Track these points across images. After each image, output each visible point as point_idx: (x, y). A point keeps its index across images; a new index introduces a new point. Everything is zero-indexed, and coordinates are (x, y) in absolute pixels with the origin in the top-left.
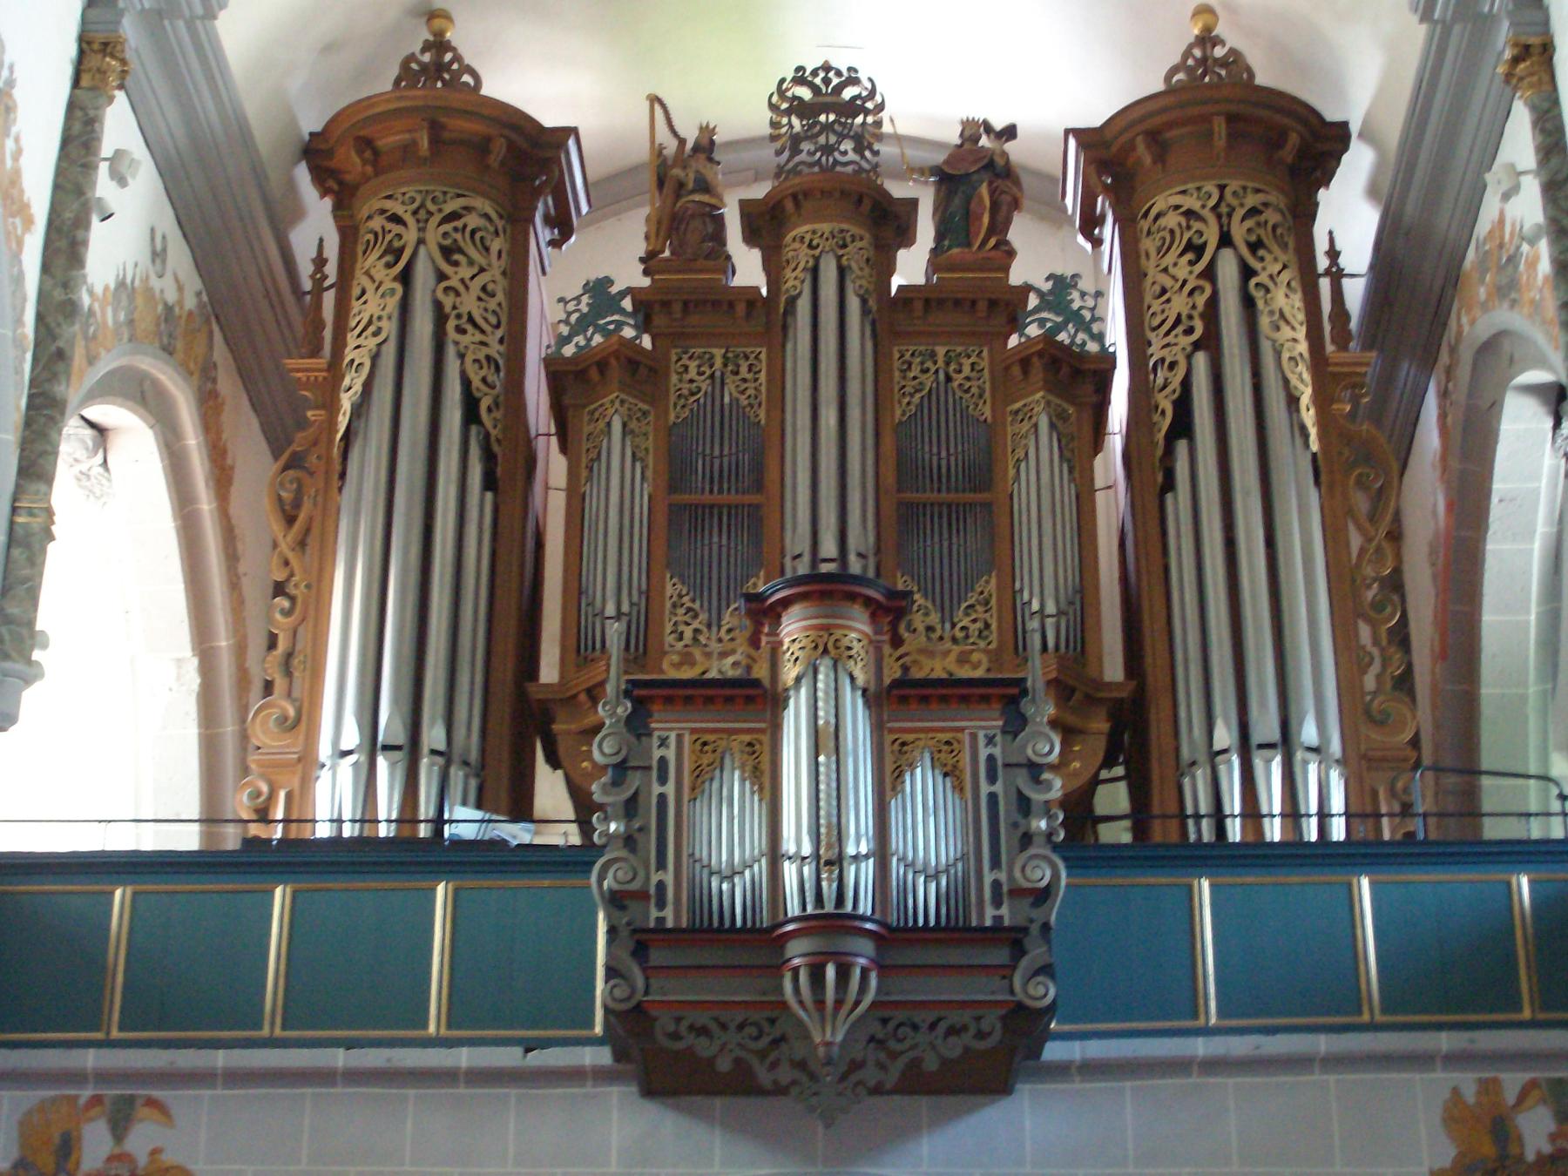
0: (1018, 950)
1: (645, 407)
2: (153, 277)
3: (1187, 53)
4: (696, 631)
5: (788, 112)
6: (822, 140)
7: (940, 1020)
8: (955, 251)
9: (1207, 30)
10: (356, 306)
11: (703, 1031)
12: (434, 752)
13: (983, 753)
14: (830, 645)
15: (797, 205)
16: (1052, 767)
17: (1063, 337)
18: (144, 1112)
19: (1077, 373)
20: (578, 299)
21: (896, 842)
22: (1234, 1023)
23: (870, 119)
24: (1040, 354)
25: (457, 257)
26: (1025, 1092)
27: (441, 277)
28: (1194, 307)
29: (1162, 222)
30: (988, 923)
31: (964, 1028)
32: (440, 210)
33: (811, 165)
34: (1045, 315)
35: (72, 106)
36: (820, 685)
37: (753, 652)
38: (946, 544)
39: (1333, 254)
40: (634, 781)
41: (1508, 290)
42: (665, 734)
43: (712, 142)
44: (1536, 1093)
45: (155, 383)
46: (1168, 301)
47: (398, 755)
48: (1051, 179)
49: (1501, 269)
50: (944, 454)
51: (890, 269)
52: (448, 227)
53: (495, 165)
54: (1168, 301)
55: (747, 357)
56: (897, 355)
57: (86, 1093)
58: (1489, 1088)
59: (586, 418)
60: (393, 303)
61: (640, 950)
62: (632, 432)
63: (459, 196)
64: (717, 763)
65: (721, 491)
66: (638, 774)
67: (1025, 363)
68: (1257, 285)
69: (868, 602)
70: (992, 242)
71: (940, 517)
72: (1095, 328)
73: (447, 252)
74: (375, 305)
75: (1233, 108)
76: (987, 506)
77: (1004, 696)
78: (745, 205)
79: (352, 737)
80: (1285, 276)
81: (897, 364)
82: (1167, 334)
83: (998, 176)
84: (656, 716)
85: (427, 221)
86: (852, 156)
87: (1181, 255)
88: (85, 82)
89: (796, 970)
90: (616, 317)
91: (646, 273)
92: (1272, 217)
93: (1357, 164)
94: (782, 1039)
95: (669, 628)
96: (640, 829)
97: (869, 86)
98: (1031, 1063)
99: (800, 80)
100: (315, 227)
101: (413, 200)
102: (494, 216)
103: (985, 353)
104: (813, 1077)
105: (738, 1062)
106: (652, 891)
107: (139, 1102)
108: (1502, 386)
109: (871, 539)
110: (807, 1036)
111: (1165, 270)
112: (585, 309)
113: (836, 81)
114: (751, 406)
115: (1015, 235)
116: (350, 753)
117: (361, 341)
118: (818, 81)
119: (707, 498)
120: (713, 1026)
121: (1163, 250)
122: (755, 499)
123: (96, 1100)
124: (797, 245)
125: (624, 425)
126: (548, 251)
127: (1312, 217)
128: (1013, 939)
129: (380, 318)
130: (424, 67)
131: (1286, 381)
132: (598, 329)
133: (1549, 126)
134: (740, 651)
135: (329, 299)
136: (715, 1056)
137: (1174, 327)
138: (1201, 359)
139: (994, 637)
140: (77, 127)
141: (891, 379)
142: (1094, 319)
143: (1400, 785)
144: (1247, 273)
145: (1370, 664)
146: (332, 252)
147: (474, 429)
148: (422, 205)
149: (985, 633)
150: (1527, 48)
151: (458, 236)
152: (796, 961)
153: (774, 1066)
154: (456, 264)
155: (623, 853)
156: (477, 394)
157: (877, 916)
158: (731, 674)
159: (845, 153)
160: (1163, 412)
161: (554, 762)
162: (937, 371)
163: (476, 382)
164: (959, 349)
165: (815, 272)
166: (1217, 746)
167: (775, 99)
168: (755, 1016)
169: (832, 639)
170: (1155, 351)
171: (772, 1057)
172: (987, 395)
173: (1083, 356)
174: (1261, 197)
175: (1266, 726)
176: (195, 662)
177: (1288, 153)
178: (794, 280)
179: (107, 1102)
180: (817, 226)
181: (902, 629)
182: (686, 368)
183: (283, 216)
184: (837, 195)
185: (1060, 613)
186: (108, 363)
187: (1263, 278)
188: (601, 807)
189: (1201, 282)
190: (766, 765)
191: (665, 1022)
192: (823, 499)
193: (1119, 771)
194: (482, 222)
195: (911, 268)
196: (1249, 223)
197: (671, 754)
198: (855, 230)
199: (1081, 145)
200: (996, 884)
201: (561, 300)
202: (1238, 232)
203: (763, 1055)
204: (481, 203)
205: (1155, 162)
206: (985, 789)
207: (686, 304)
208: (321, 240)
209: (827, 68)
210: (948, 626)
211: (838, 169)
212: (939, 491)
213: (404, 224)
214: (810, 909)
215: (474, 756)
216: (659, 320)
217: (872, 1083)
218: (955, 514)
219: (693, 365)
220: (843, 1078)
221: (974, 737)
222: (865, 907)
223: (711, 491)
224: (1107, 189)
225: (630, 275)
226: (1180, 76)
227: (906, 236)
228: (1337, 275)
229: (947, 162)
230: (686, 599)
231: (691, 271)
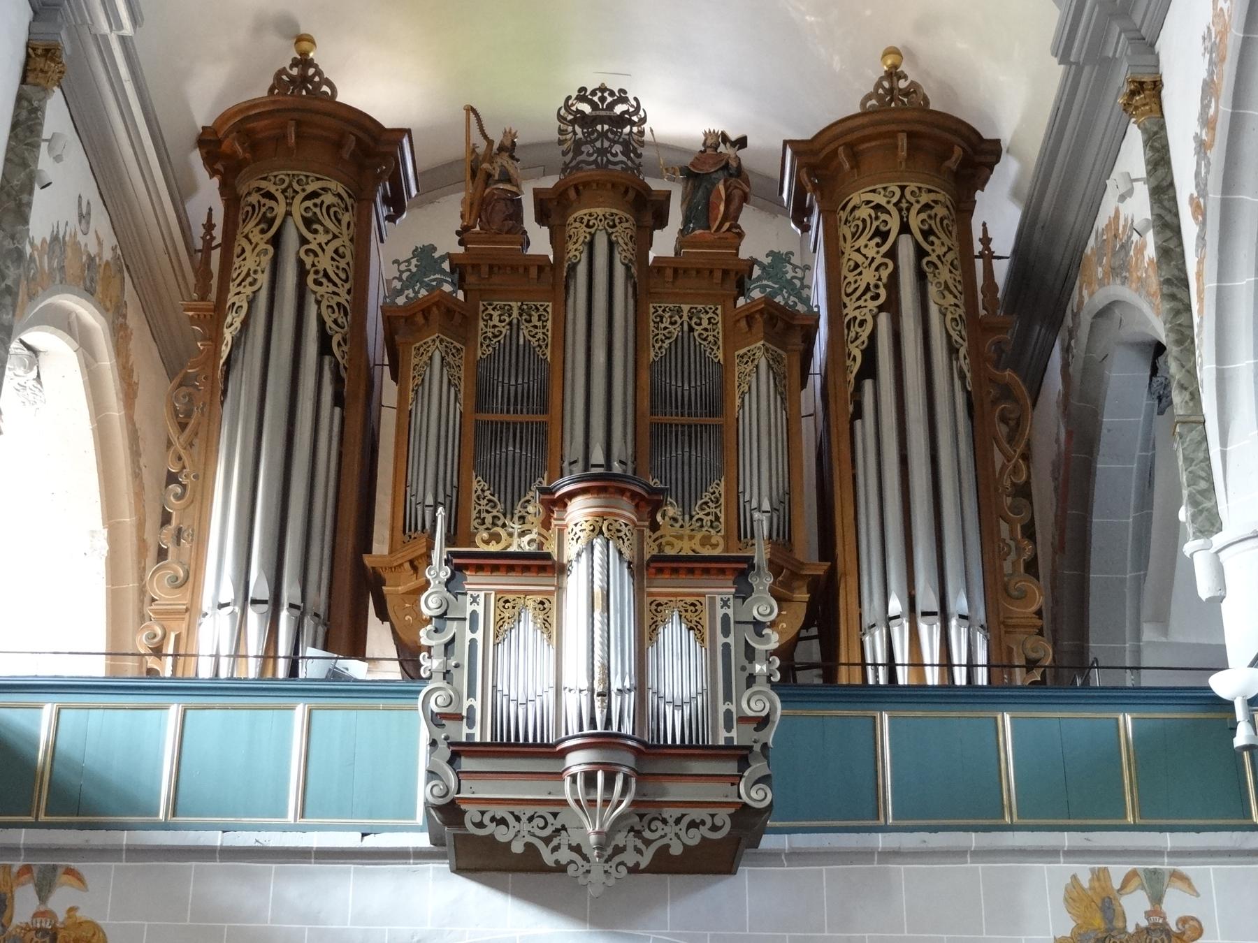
0: (744, 762)
1: (459, 346)
2: (80, 234)
3: (879, 85)
4: (494, 517)
5: (572, 123)
6: (598, 144)
7: (683, 815)
8: (698, 232)
9: (895, 67)
10: (237, 262)
11: (502, 822)
12: (292, 606)
13: (720, 612)
14: (604, 529)
15: (577, 192)
16: (773, 625)
17: (779, 299)
18: (65, 878)
19: (789, 327)
20: (408, 261)
21: (651, 681)
22: (905, 823)
23: (635, 129)
24: (761, 312)
25: (316, 226)
26: (744, 871)
27: (304, 241)
28: (880, 279)
29: (857, 213)
30: (722, 742)
31: (703, 823)
32: (304, 190)
34: (765, 282)
35: (20, 98)
36: (595, 558)
37: (544, 532)
38: (687, 455)
39: (986, 240)
40: (452, 628)
41: (1120, 270)
42: (475, 593)
43: (513, 144)
44: (1135, 882)
46: (860, 273)
47: (265, 607)
48: (769, 179)
49: (1115, 253)
50: (686, 387)
52: (309, 203)
53: (346, 156)
54: (860, 273)
55: (537, 309)
56: (653, 310)
57: (17, 864)
58: (1100, 876)
59: (414, 353)
60: (266, 261)
61: (453, 760)
62: (449, 364)
63: (318, 179)
64: (516, 617)
65: (515, 411)
66: (455, 623)
67: (750, 319)
68: (928, 263)
69: (634, 495)
70: (727, 225)
71: (683, 435)
72: (805, 292)
73: (308, 222)
76: (719, 428)
77: (735, 569)
78: (537, 193)
79: (227, 594)
80: (950, 256)
81: (652, 317)
82: (859, 299)
83: (731, 175)
84: (470, 579)
85: (293, 198)
86: (621, 157)
87: (870, 239)
88: (29, 80)
89: (574, 777)
90: (437, 276)
92: (940, 211)
93: (1007, 173)
94: (564, 828)
95: (474, 514)
96: (457, 666)
97: (634, 103)
98: (753, 850)
99: (582, 98)
101: (283, 181)
102: (345, 196)
103: (719, 312)
105: (529, 846)
106: (464, 714)
107: (60, 871)
109: (630, 451)
111: (858, 250)
112: (414, 270)
113: (609, 99)
114: (540, 346)
115: (741, 222)
116: (227, 605)
117: (240, 289)
118: (596, 99)
119: (505, 417)
120: (510, 819)
121: (856, 236)
122: (541, 418)
123: (27, 869)
124: (577, 224)
125: (443, 359)
126: (385, 225)
127: (971, 212)
128: (742, 756)
129: (255, 272)
130: (293, 80)
131: (949, 336)
132: (424, 285)
133: (1157, 145)
134: (535, 530)
135: (216, 255)
136: (510, 842)
137: (864, 294)
138: (884, 318)
139: (722, 526)
140: (24, 114)
141: (648, 326)
142: (803, 287)
143: (1028, 646)
144: (920, 253)
145: (1009, 554)
146: (218, 219)
147: (327, 359)
148: (290, 186)
149: (716, 524)
150: (1142, 83)
151: (317, 210)
152: (573, 770)
153: (556, 849)
154: (315, 232)
155: (443, 684)
156: (330, 332)
157: (636, 736)
158: (527, 549)
159: (615, 155)
160: (854, 359)
161: (383, 615)
162: (682, 324)
163: (329, 323)
164: (700, 307)
165: (591, 245)
166: (892, 613)
167: (563, 112)
168: (542, 810)
169: (606, 523)
170: (850, 312)
171: (555, 842)
172: (720, 343)
173: (794, 314)
174: (933, 196)
175: (927, 599)
176: (105, 532)
177: (952, 163)
178: (575, 250)
179: (35, 871)
180: (593, 210)
181: (659, 518)
182: (491, 316)
183: (181, 192)
184: (609, 186)
185: (774, 509)
188: (429, 649)
189: (886, 260)
190: (554, 621)
194: (336, 200)
195: (664, 244)
196: (923, 216)
197: (480, 610)
198: (621, 214)
199: (795, 153)
200: (728, 713)
201: (394, 262)
202: (915, 222)
203: (547, 841)
204: (334, 185)
205: (852, 168)
206: (721, 640)
207: (491, 267)
208: (210, 209)
209: (603, 89)
210: (687, 517)
211: (610, 167)
212: (682, 415)
213: (276, 200)
214: (586, 731)
215: (322, 610)
216: (471, 279)
217: (630, 864)
218: (694, 434)
219: (495, 314)
221: (712, 600)
222: (627, 729)
223: (508, 411)
224: (816, 188)
225: (449, 245)
226: (874, 102)
227: (661, 221)
228: (988, 256)
229: (692, 164)
230: (487, 493)
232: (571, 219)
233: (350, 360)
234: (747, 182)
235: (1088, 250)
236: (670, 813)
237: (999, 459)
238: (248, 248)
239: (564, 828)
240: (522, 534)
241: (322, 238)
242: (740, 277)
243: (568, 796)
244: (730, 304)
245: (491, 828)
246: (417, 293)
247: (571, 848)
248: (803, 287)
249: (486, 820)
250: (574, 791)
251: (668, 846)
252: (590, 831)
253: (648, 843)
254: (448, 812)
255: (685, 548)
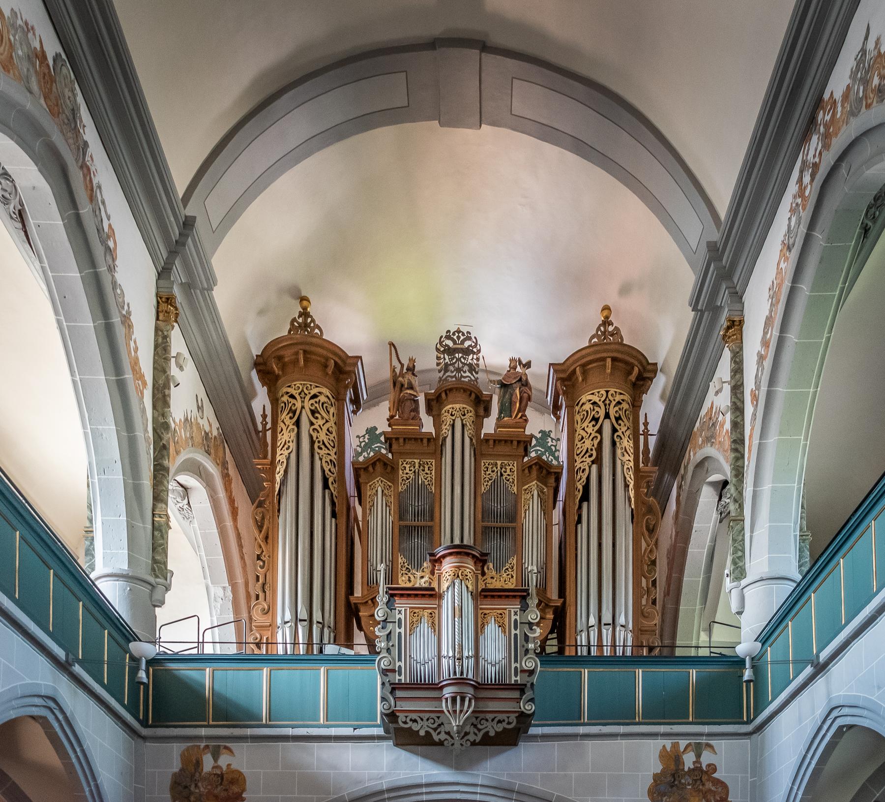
2: (199, 419)
10: (279, 436)
11: (415, 721)
15: (446, 394)
17: (544, 457)
23: (475, 357)
27: (312, 424)
29: (584, 407)
31: (504, 721)
33: (452, 377)
45: (204, 467)
51: (481, 426)
60: (293, 435)
70: (520, 415)
74: (286, 436)
75: (615, 355)
89: (447, 699)
91: (390, 425)
94: (442, 724)
100: (261, 401)
104: (452, 738)
105: (427, 732)
108: (703, 481)
110: (451, 723)
111: (584, 429)
126: (351, 415)
135: (269, 433)
136: (418, 731)
144: (614, 430)
146: (269, 412)
152: (447, 696)
153: (439, 733)
168: (433, 715)
170: (578, 465)
171: (439, 730)
178: (446, 429)
183: (248, 396)
186: (184, 456)
187: (620, 433)
191: (401, 717)
192: (455, 519)
193: (555, 635)
203: (435, 729)
220: (463, 737)
224: (564, 393)
225: (383, 427)
231: (405, 425)
232: (443, 411)
233: (338, 492)
234: (530, 389)
235: (695, 429)
236: (490, 716)
237: (644, 545)
238: (284, 428)
239: (442, 724)
240: (422, 577)
241: (321, 422)
242: (525, 444)
243: (444, 709)
244: (520, 460)
245: (410, 724)
246: (369, 454)
247: (446, 733)
248: (556, 450)
249: (408, 720)
250: (447, 706)
251: (488, 732)
252: (455, 724)
253: (480, 730)
254: (391, 716)
255: (497, 584)
